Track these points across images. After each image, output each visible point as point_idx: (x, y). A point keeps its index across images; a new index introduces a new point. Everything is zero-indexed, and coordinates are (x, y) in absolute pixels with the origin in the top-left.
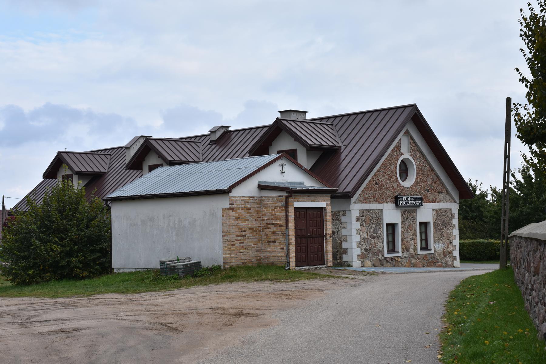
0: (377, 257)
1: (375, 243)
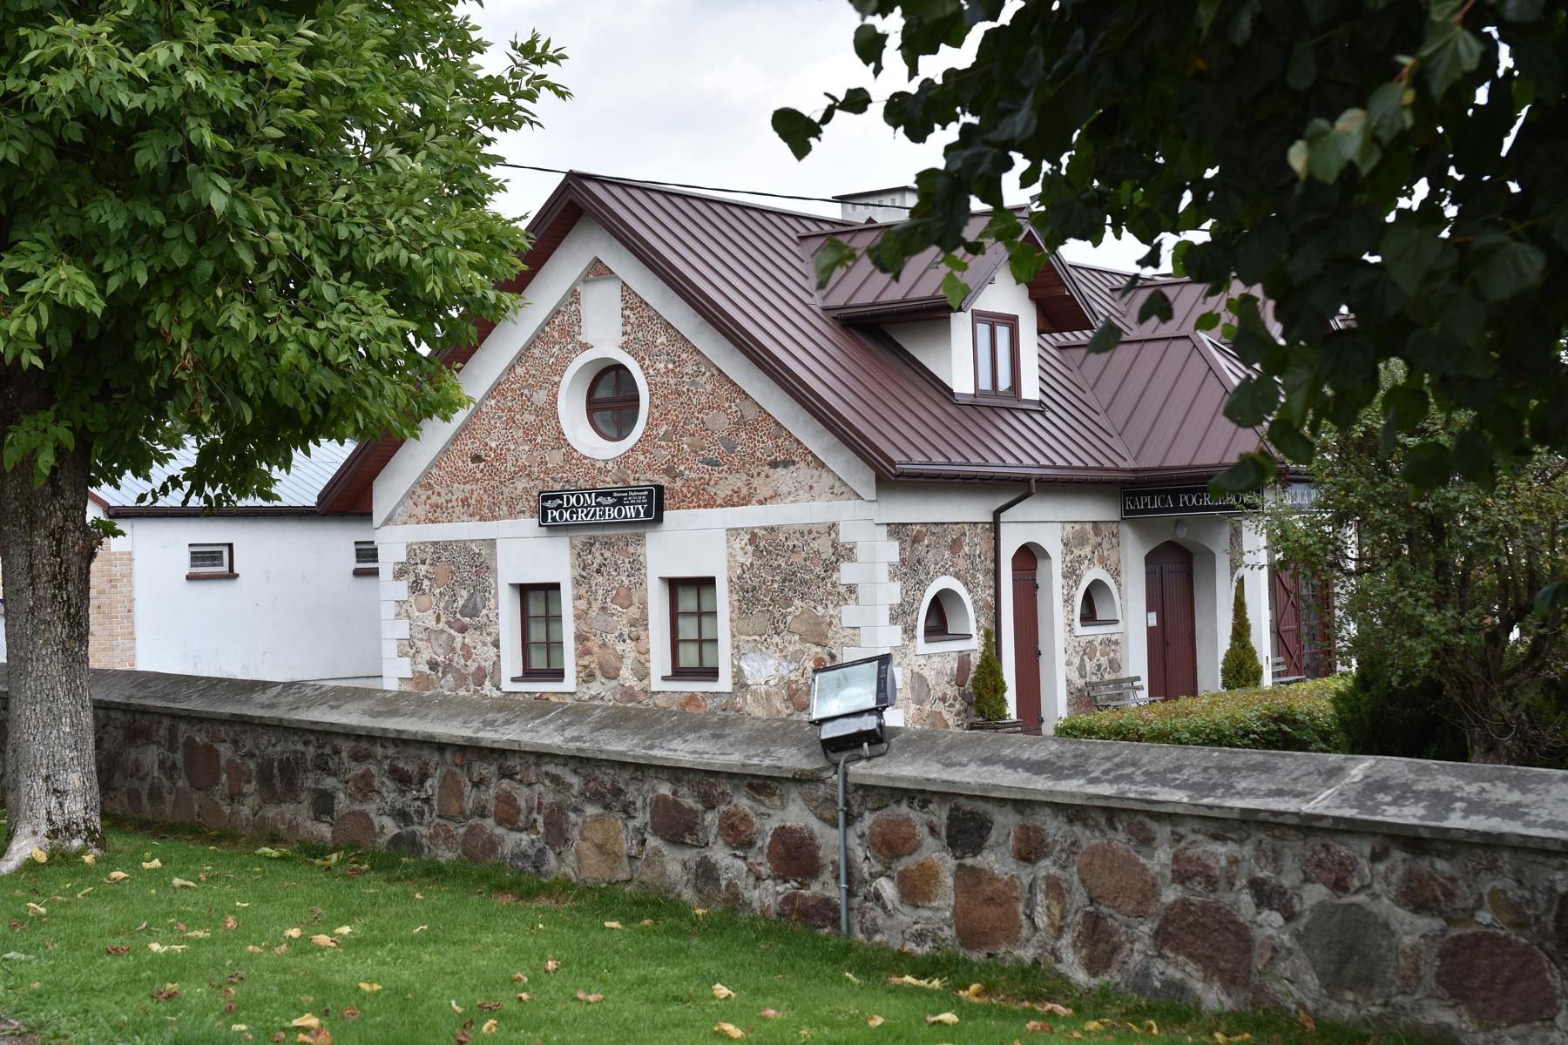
0: (476, 691)
1: (464, 644)
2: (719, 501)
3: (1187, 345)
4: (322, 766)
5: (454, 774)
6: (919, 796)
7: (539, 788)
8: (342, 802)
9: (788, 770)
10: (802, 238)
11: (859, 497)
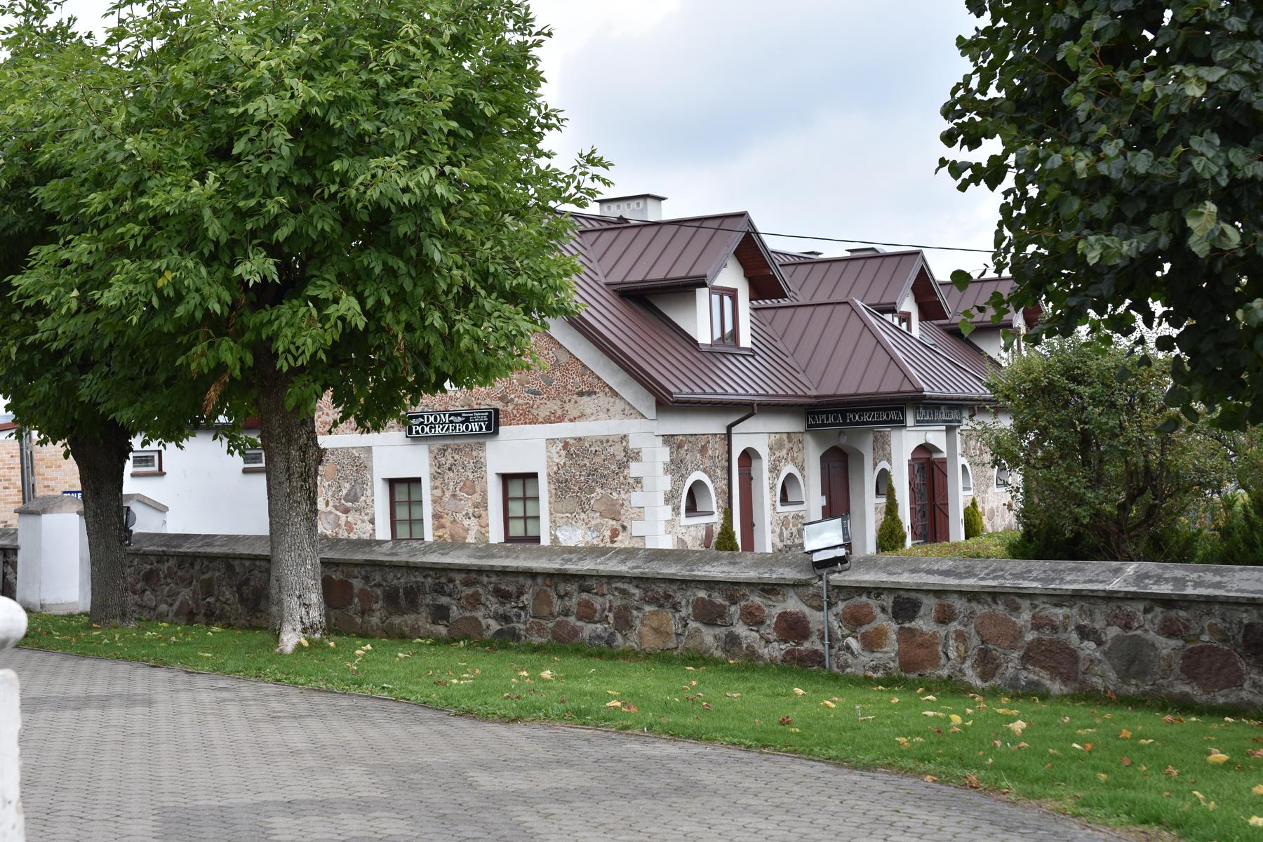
1: (347, 523)
2: (540, 420)
3: (846, 308)
4: (439, 590)
5: (545, 591)
6: (875, 591)
7: (610, 597)
8: (455, 612)
9: (790, 580)
10: (581, 232)
11: (643, 416)
